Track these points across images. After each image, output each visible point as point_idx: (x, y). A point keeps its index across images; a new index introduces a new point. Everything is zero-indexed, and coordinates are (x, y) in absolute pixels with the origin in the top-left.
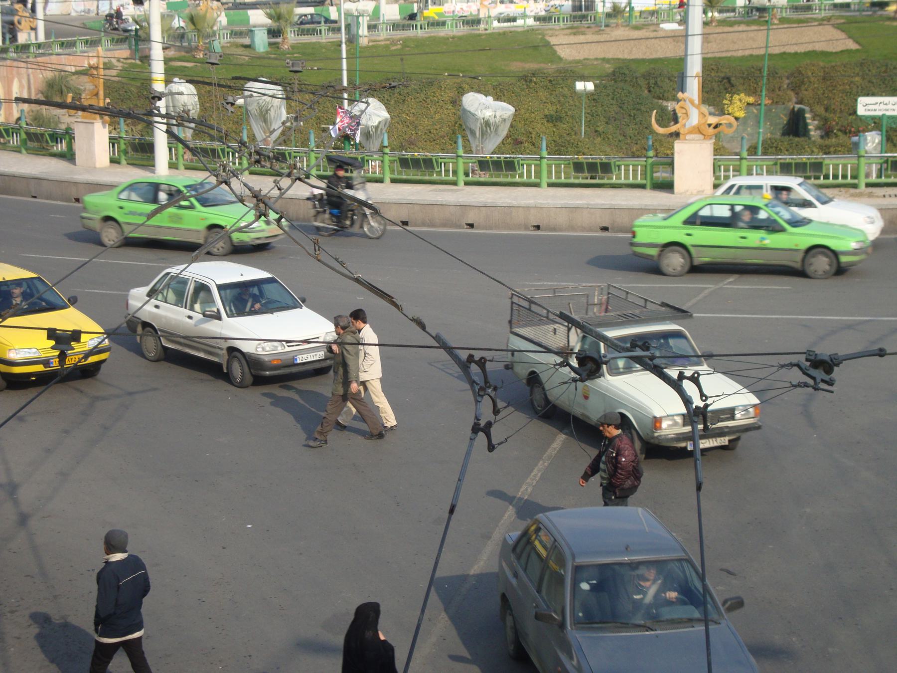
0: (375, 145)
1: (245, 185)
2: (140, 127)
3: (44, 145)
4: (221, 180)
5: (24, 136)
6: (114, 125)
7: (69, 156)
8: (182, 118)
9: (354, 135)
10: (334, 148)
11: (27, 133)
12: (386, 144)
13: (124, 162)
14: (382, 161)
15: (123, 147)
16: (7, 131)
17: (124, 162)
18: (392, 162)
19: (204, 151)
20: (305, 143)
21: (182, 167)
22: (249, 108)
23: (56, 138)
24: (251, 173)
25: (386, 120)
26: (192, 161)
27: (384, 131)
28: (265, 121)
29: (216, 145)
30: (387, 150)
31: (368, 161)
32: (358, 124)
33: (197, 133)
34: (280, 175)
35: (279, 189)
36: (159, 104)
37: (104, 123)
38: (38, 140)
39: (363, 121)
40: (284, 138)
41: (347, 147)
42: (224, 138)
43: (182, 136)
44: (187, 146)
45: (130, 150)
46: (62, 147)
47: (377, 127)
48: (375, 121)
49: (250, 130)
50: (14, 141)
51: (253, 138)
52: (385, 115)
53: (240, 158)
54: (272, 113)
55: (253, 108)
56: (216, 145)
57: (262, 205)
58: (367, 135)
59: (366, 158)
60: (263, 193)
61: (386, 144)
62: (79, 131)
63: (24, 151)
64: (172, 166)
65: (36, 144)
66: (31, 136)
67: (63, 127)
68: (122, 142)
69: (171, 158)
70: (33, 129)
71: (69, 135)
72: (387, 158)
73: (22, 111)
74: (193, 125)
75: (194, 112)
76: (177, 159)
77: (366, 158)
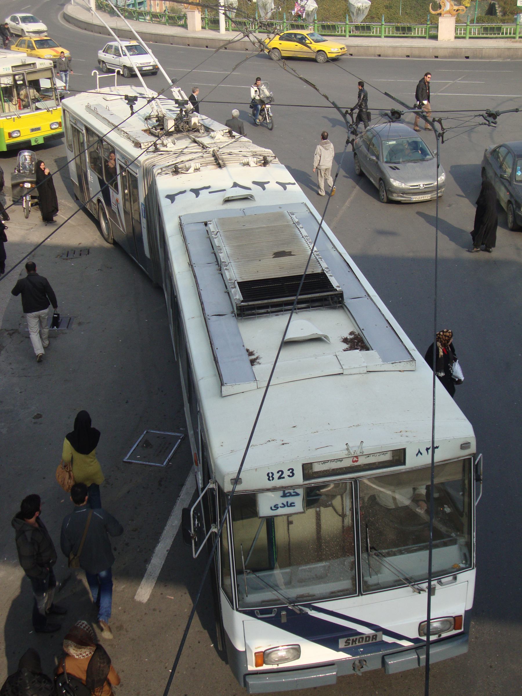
0: (311, 20)
1: (255, 37)
2: (213, 13)
3: (175, 21)
4: (245, 35)
5: (167, 18)
6: (203, 12)
7: (185, 26)
9: (302, 15)
10: (294, 21)
11: (168, 17)
12: (316, 19)
13: (207, 28)
14: (314, 27)
15: (207, 22)
17: (207, 28)
18: (318, 27)
19: (240, 23)
20: (282, 19)
22: (259, 4)
23: (180, 18)
24: (259, 32)
25: (316, 8)
26: (235, 27)
27: (315, 13)
28: (265, 9)
29: (244, 20)
30: (316, 22)
31: (308, 26)
32: (304, 10)
33: (238, 15)
34: (270, 33)
35: (269, 39)
37: (199, 11)
38: (173, 19)
39: (306, 9)
40: (273, 18)
41: (299, 20)
42: (248, 17)
43: (230, 16)
44: (232, 21)
45: (209, 23)
46: (182, 22)
47: (312, 11)
48: (311, 9)
49: (259, 13)
50: (164, 20)
51: (260, 16)
52: (316, 6)
53: (255, 26)
54: (268, 5)
56: (244, 20)
57: (262, 46)
58: (308, 15)
59: (307, 25)
60: (262, 40)
61: (316, 19)
62: (189, 15)
63: (167, 24)
64: (227, 30)
65: (172, 21)
66: (170, 18)
67: (183, 13)
68: (206, 19)
69: (226, 26)
70: (171, 15)
71: (185, 17)
72: (316, 25)
73: (166, 7)
74: (235, 11)
76: (229, 26)
77: (307, 25)
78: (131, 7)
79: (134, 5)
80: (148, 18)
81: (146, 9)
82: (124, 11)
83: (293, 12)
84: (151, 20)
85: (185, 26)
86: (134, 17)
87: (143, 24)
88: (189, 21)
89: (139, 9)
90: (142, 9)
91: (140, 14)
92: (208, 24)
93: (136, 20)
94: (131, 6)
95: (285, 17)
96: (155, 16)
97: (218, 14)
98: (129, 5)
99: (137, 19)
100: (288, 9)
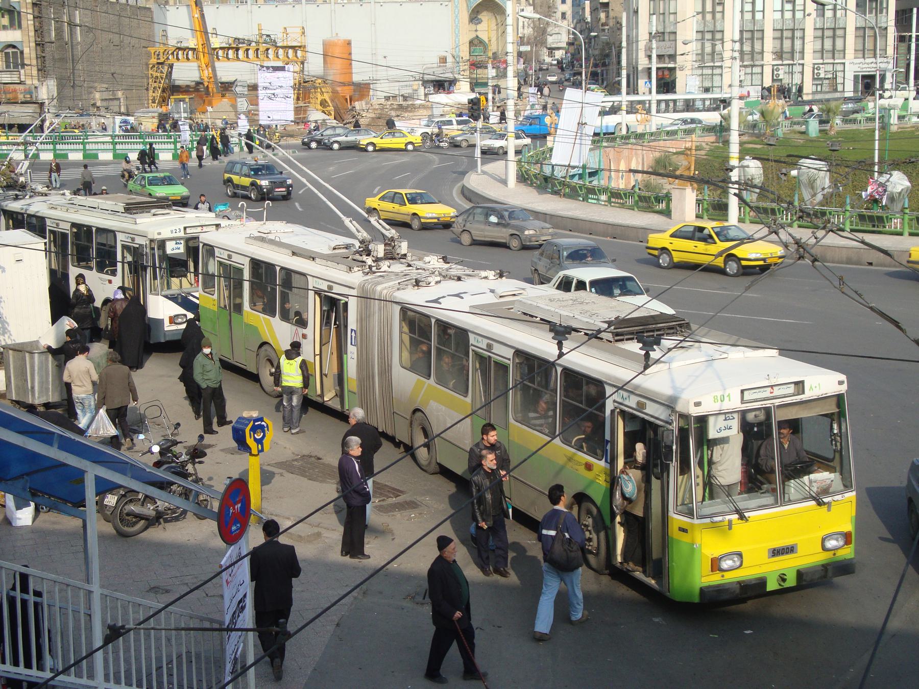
0: (897, 207)
1: (790, 235)
2: (719, 192)
3: (650, 204)
4: (771, 230)
5: (637, 198)
6: (700, 191)
7: (667, 213)
8: (746, 185)
9: (881, 199)
10: (865, 209)
11: (639, 197)
12: (906, 206)
13: (706, 217)
14: (903, 219)
15: (706, 206)
16: (625, 194)
18: (911, 220)
19: (765, 211)
20: (842, 205)
21: (747, 221)
22: (801, 178)
23: (658, 200)
24: (800, 226)
25: (908, 188)
26: (755, 217)
27: (906, 196)
28: (812, 188)
29: (774, 205)
30: (907, 211)
31: (891, 219)
32: (885, 191)
33: (761, 196)
34: (817, 228)
35: (816, 238)
36: (731, 174)
37: (693, 189)
38: (646, 201)
39: (889, 189)
40: (827, 200)
41: (875, 208)
42: (779, 200)
43: (748, 200)
44: (751, 208)
45: (710, 208)
46: (662, 206)
47: (900, 193)
48: (899, 189)
49: (800, 195)
50: (630, 202)
51: (802, 200)
52: (908, 184)
53: (792, 215)
54: (818, 182)
55: (804, 179)
56: (774, 205)
57: (801, 250)
58: (892, 199)
59: (890, 217)
60: (803, 241)
61: (906, 206)
62: (675, 195)
63: (636, 209)
64: (741, 220)
67: (665, 192)
68: (705, 202)
69: (740, 215)
70: (643, 194)
71: (668, 198)
72: (907, 217)
73: (636, 180)
74: (758, 191)
75: (758, 181)
76: (744, 215)
77: (890, 217)
78: (576, 180)
79: (581, 176)
80: (603, 197)
81: (602, 182)
82: (564, 185)
83: (863, 193)
84: (609, 201)
85: (667, 213)
86: (580, 196)
87: (595, 208)
88: (673, 205)
89: (590, 182)
90: (595, 183)
91: (591, 191)
92: (707, 210)
93: (583, 200)
94: (577, 177)
95: (848, 201)
96: (615, 195)
97: (725, 192)
98: (573, 176)
99: (585, 199)
100: (855, 188)
